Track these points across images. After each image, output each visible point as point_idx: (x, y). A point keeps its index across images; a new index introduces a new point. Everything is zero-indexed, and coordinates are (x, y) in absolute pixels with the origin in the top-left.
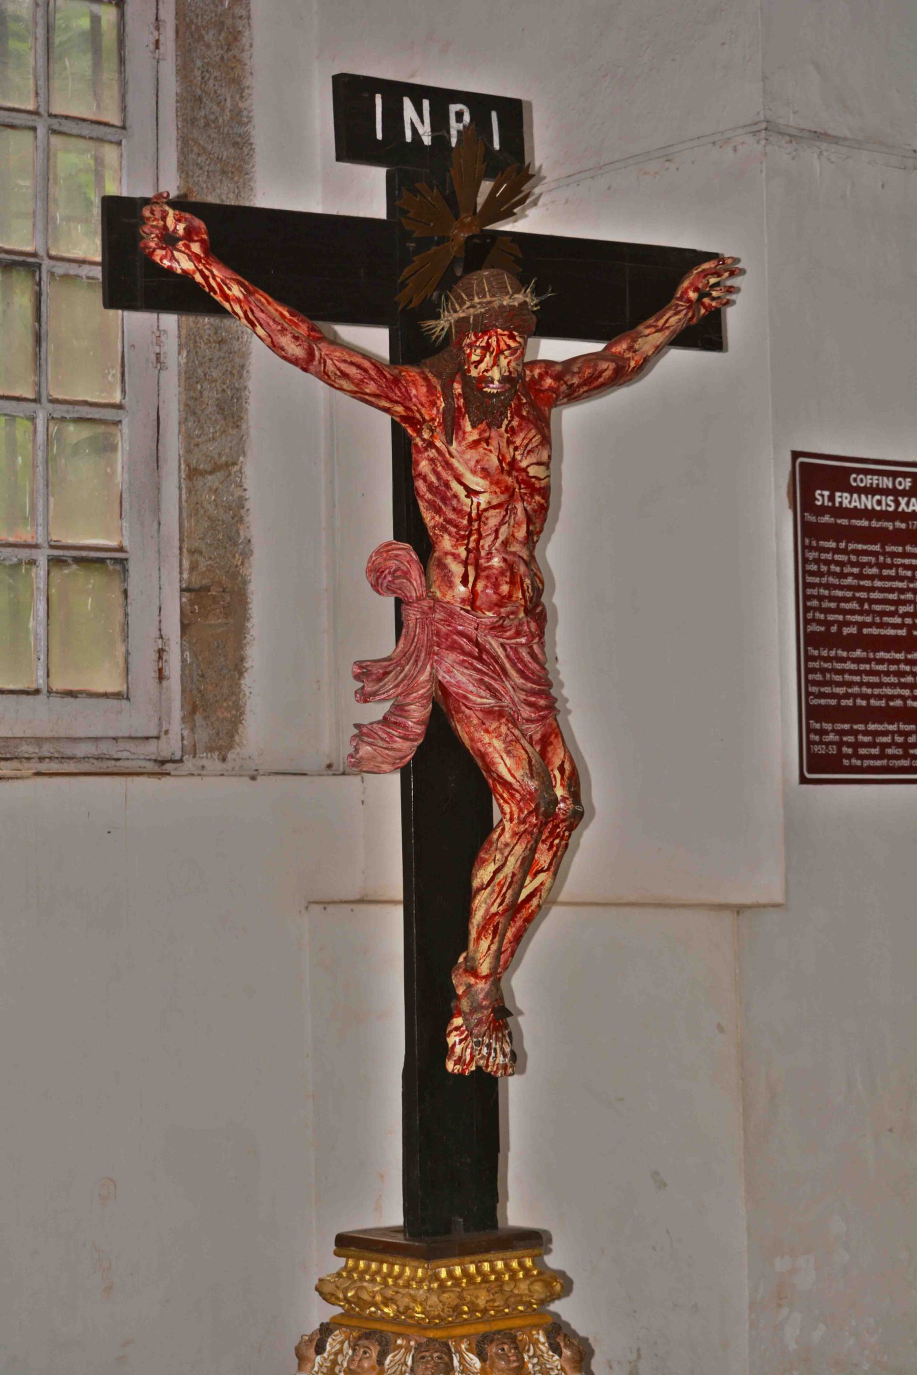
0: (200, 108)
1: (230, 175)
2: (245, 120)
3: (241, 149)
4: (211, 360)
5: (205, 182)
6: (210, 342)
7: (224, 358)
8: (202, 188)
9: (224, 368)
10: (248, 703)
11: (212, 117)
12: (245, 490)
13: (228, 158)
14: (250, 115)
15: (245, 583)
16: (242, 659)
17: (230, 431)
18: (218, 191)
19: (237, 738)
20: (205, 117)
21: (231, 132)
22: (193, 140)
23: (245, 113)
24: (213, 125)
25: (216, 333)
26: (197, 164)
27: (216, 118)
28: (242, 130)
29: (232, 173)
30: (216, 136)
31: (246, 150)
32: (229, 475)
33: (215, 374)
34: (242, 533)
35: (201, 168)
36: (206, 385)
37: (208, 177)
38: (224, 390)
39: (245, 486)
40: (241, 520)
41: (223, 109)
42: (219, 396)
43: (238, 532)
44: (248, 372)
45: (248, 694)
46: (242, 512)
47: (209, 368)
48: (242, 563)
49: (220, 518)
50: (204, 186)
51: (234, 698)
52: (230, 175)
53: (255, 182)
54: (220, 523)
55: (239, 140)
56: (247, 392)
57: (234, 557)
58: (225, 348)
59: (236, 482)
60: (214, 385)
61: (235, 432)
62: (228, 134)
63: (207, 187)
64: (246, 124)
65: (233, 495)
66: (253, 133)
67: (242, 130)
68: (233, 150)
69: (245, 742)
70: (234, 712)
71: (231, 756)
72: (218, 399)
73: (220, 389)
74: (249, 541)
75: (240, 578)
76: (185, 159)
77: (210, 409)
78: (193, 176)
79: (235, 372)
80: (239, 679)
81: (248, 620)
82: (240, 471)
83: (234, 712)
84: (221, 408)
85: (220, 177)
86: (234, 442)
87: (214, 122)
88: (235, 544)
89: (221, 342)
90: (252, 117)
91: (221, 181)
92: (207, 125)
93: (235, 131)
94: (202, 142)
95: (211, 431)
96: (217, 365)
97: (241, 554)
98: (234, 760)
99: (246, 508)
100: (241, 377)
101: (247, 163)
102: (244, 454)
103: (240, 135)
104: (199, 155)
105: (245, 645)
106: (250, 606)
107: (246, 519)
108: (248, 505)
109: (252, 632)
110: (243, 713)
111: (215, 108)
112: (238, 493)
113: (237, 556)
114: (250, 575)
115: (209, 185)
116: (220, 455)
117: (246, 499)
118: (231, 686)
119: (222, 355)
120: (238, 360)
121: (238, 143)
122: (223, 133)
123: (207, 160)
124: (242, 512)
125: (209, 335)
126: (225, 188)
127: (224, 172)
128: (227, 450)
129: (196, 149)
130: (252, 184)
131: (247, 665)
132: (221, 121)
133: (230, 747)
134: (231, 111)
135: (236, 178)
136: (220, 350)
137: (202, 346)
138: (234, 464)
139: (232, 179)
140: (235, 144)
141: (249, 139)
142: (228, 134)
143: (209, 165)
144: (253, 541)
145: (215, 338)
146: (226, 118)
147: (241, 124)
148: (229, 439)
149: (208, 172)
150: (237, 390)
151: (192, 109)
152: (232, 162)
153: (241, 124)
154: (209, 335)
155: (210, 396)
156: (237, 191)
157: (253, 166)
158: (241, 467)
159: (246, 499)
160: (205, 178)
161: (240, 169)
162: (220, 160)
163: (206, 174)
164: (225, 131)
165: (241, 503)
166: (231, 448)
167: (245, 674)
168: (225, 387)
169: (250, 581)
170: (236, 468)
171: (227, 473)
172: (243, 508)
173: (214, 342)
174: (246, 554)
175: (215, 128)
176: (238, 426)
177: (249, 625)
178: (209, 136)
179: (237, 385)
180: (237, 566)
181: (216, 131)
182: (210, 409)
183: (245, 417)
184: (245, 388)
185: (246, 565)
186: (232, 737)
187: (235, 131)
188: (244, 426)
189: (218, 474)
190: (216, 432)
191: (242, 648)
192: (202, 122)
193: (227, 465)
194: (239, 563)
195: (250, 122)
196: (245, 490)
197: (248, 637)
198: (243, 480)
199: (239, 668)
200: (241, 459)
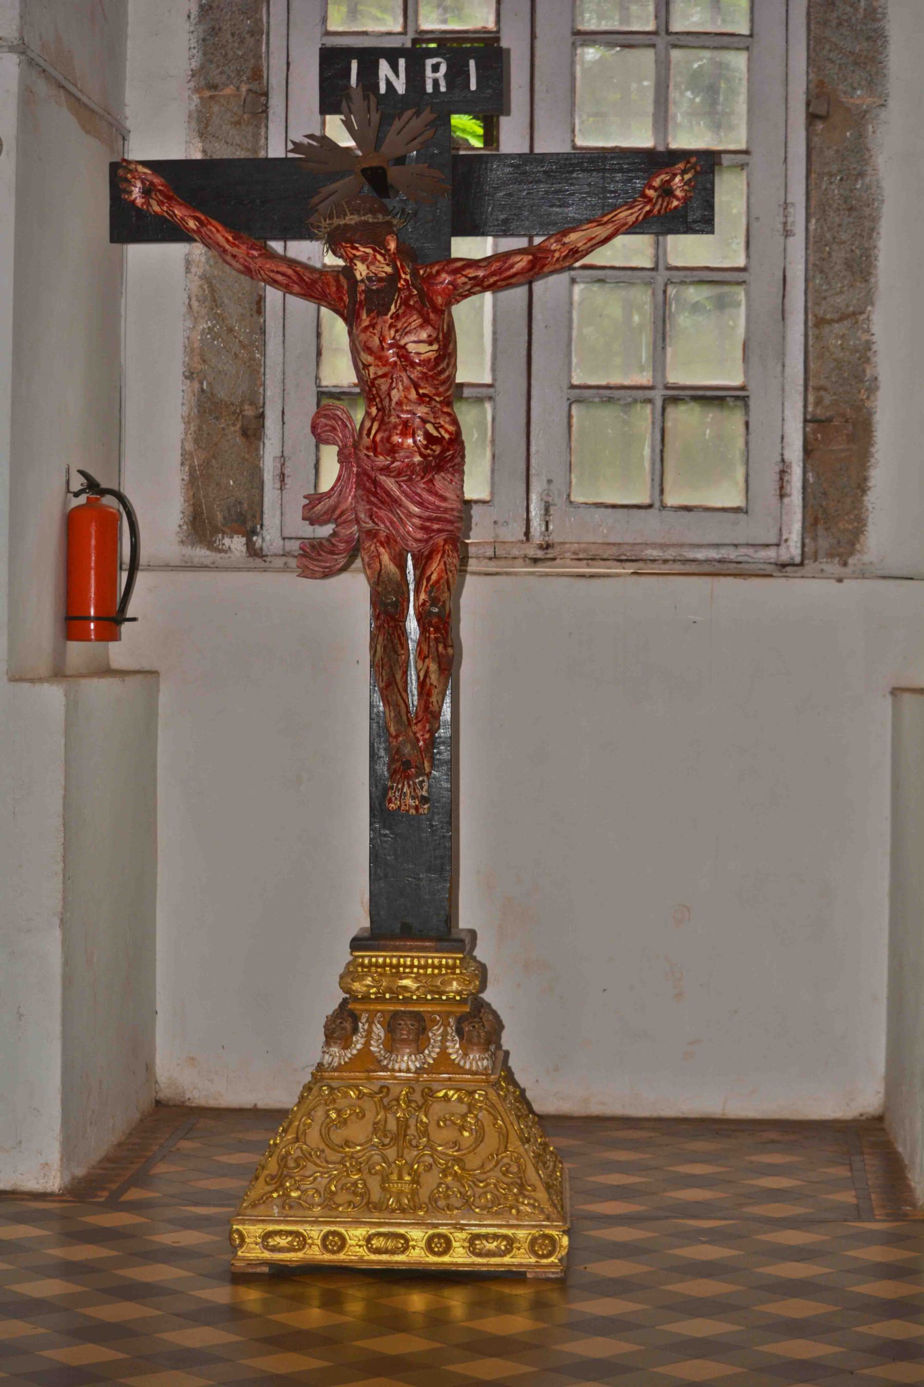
0: (832, 11)
1: (862, 65)
2: (879, 16)
3: (875, 42)
4: (840, 225)
5: (837, 74)
6: (839, 210)
7: (853, 223)
8: (834, 79)
9: (854, 231)
10: (871, 516)
11: (845, 17)
12: (873, 335)
13: (861, 50)
14: (885, 11)
15: (870, 414)
16: (865, 479)
17: (858, 284)
18: (850, 80)
19: (858, 546)
20: (838, 18)
21: (864, 28)
22: (825, 38)
23: (880, 10)
24: (846, 24)
25: (845, 202)
26: (829, 59)
27: (850, 18)
28: (876, 25)
29: (865, 63)
30: (848, 33)
31: (879, 43)
32: (857, 322)
33: (844, 237)
34: (868, 372)
35: (833, 62)
36: (835, 247)
37: (840, 68)
38: (852, 251)
39: (873, 331)
40: (868, 360)
41: (857, 10)
42: (848, 255)
43: (864, 371)
44: (878, 233)
45: (870, 509)
46: (869, 354)
47: (838, 232)
48: (868, 398)
49: (845, 359)
50: (836, 77)
51: (856, 512)
52: (862, 65)
53: (889, 69)
54: (846, 364)
55: (873, 34)
56: (876, 251)
57: (859, 392)
58: (854, 214)
59: (863, 328)
60: (842, 246)
61: (863, 286)
62: (861, 30)
63: (839, 79)
64: (879, 20)
65: (859, 339)
66: (887, 27)
67: (876, 25)
68: (865, 44)
69: (866, 550)
70: (856, 524)
71: (851, 561)
72: (846, 259)
73: (848, 250)
74: (876, 379)
75: (865, 410)
76: (817, 55)
77: (838, 267)
78: (823, 70)
79: (865, 234)
80: (862, 496)
81: (873, 445)
82: (868, 319)
83: (856, 524)
84: (848, 265)
85: (852, 68)
86: (863, 294)
87: (846, 21)
88: (862, 381)
89: (851, 209)
90: (887, 13)
91: (853, 71)
92: (840, 24)
93: (869, 26)
94: (834, 39)
95: (839, 285)
96: (847, 229)
97: (867, 390)
98: (855, 565)
99: (873, 350)
100: (870, 237)
101: (881, 53)
102: (872, 304)
103: (875, 30)
104: (830, 51)
105: (869, 467)
106: (875, 434)
107: (874, 359)
108: (874, 347)
109: (876, 456)
110: (865, 525)
111: (848, 9)
112: (865, 337)
113: (863, 391)
114: (876, 407)
115: (841, 75)
116: (848, 306)
117: (874, 343)
118: (853, 502)
119: (851, 220)
120: (867, 224)
121: (871, 37)
122: (856, 30)
123: (839, 54)
124: (869, 354)
125: (839, 204)
126: (857, 77)
127: (856, 63)
128: (855, 302)
129: (828, 47)
130: (885, 71)
131: (870, 484)
132: (854, 20)
133: (851, 554)
134: (865, 10)
135: (868, 68)
136: (849, 216)
137: (832, 214)
138: (862, 313)
139: (865, 68)
140: (868, 38)
141: (883, 33)
142: (861, 30)
143: (841, 59)
144: (880, 378)
145: (844, 206)
146: (860, 15)
147: (874, 20)
148: (857, 292)
149: (840, 65)
150: (866, 249)
151: (825, 12)
152: (865, 53)
153: (874, 20)
154: (839, 204)
155: (839, 256)
156: (869, 78)
157: (887, 56)
158: (869, 316)
159: (874, 343)
160: (836, 70)
161: (873, 60)
162: (852, 53)
163: (837, 66)
164: (858, 28)
165: (868, 345)
166: (858, 300)
167: (868, 492)
168: (854, 248)
169: (875, 412)
170: (864, 316)
171: (854, 321)
172: (870, 350)
173: (844, 209)
174: (873, 389)
175: (848, 26)
176: (866, 281)
177: (873, 450)
178: (842, 34)
179: (866, 245)
180: (862, 400)
181: (849, 29)
182: (838, 267)
183: (874, 272)
184: (875, 247)
185: (872, 398)
186: (853, 545)
187: (869, 26)
188: (873, 280)
189: (846, 322)
190: (844, 287)
191: (865, 470)
192: (834, 23)
193: (854, 314)
194: (865, 397)
195: (884, 17)
196: (873, 335)
197: (873, 460)
198: (871, 326)
199: (862, 487)
200: (869, 308)
